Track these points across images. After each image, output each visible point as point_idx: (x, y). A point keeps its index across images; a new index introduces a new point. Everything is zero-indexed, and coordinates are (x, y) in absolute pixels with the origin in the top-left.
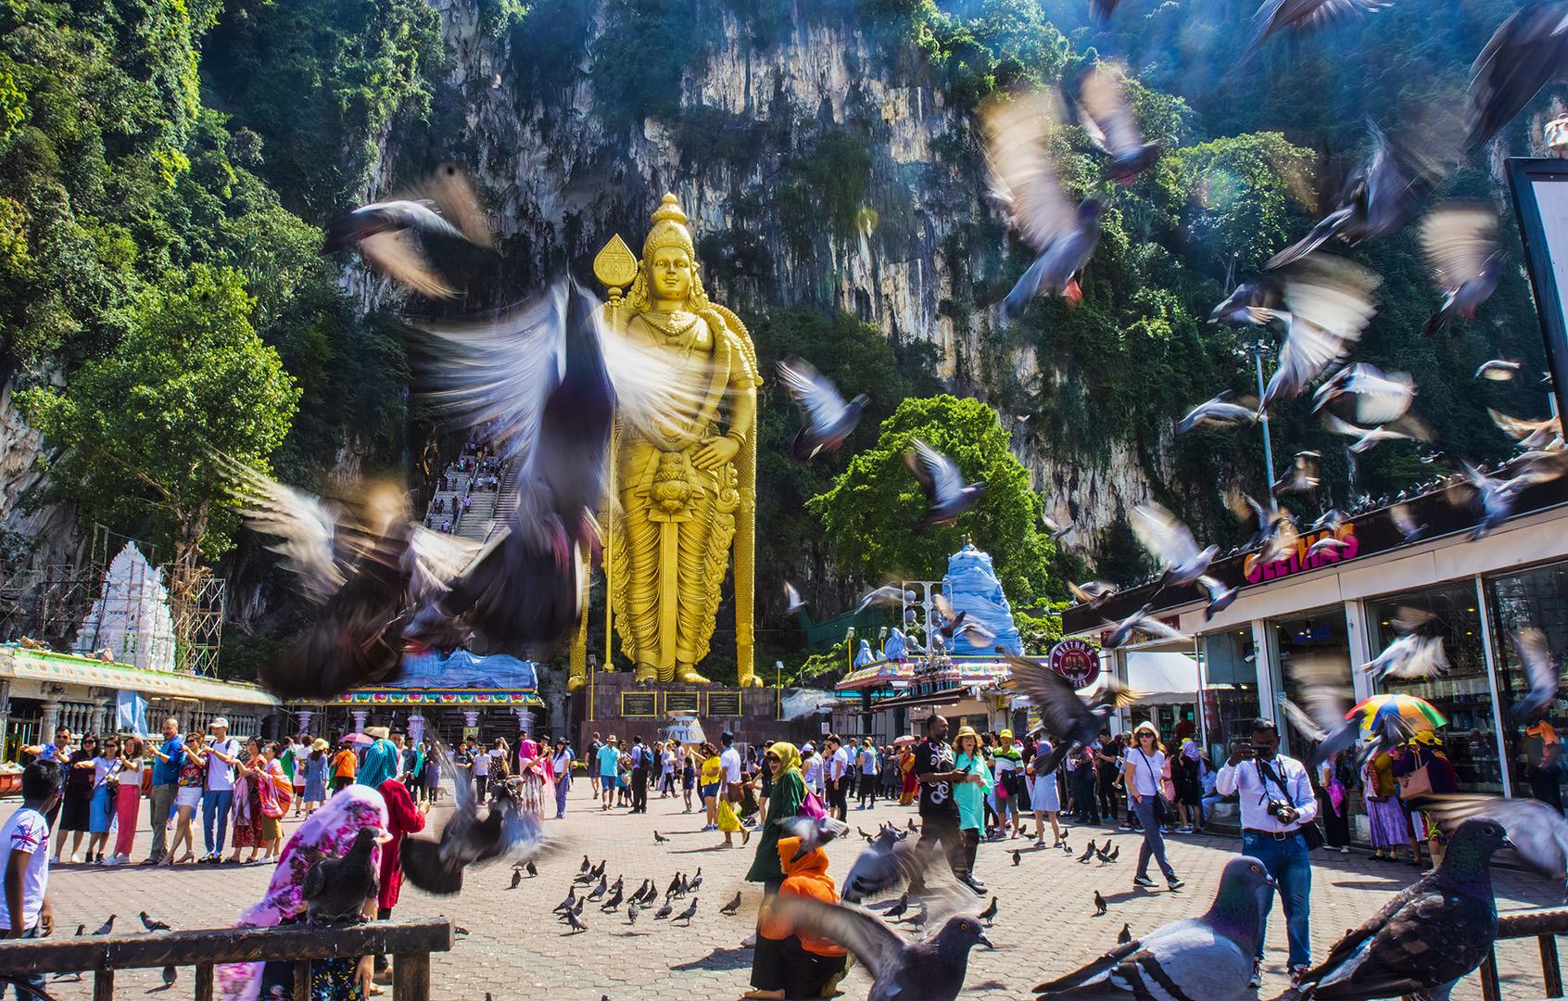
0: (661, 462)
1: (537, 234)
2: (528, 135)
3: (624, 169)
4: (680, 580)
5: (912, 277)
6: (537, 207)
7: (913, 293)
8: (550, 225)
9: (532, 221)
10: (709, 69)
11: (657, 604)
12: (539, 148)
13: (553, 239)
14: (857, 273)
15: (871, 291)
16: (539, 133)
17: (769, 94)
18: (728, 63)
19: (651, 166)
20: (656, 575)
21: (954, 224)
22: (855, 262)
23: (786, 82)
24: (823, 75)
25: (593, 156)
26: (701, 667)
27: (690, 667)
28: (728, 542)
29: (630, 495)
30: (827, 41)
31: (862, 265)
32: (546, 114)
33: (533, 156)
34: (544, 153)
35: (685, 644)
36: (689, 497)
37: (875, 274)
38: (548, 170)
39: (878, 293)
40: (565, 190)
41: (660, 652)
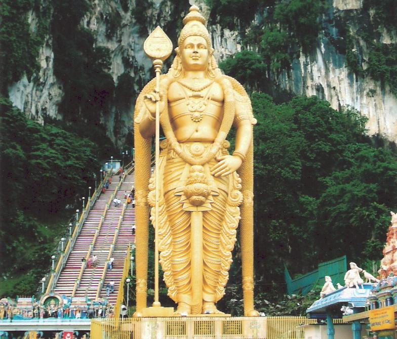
0: (190, 172)
1: (135, 73)
4: (204, 248)
6: (133, 57)
7: (351, 85)
8: (142, 68)
11: (190, 264)
12: (135, 24)
14: (316, 74)
15: (324, 85)
22: (315, 69)
27: (213, 304)
28: (236, 225)
29: (171, 195)
34: (137, 27)
35: (207, 290)
36: (209, 194)
39: (329, 86)
41: (192, 295)
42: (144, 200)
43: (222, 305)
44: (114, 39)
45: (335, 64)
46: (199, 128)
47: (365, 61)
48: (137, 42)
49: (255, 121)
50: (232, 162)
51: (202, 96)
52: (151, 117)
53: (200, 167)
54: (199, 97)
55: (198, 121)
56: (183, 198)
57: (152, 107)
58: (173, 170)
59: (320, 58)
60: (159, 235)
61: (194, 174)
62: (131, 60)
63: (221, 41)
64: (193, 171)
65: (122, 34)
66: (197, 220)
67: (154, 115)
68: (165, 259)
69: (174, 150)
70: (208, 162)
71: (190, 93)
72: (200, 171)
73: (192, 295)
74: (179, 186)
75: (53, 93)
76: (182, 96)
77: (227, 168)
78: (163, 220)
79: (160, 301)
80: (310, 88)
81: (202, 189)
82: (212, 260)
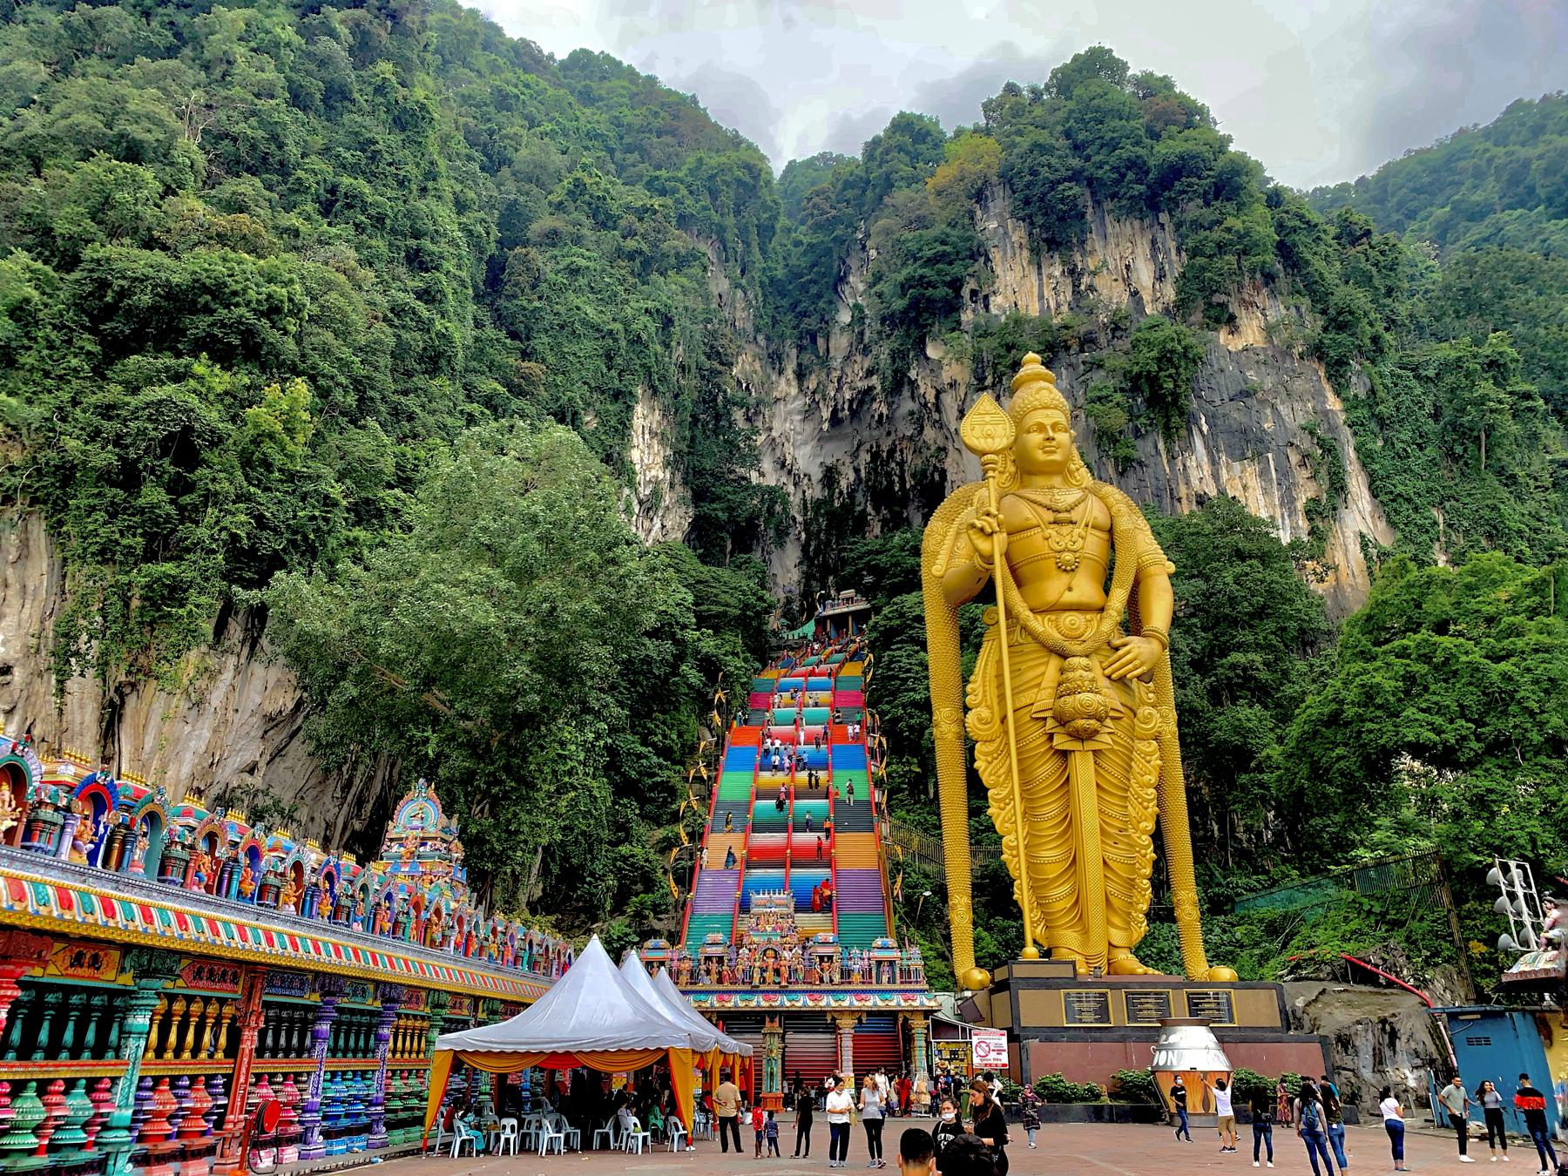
1: (795, 485)
3: (885, 412)
4: (1103, 832)
7: (1265, 492)
12: (795, 398)
14: (1194, 475)
16: (794, 383)
18: (1018, 268)
20: (1069, 822)
23: (1085, 280)
24: (1128, 267)
25: (851, 401)
26: (1143, 950)
28: (1153, 779)
30: (1128, 230)
31: (1199, 466)
33: (790, 407)
35: (1116, 920)
37: (1216, 476)
40: (822, 439)
42: (955, 728)
43: (1143, 950)
45: (1231, 456)
46: (1074, 583)
49: (1172, 568)
50: (1142, 650)
52: (978, 561)
53: (1084, 661)
56: (1050, 723)
57: (984, 545)
58: (1023, 667)
59: (1198, 443)
60: (997, 801)
61: (1071, 675)
64: (1074, 670)
65: (772, 416)
67: (989, 560)
69: (1024, 628)
70: (1096, 651)
71: (1050, 516)
72: (1087, 669)
73: (1085, 932)
74: (1043, 698)
75: (669, 524)
76: (1034, 522)
77: (1137, 662)
80: (1184, 501)
81: (1095, 705)
82: (1116, 854)
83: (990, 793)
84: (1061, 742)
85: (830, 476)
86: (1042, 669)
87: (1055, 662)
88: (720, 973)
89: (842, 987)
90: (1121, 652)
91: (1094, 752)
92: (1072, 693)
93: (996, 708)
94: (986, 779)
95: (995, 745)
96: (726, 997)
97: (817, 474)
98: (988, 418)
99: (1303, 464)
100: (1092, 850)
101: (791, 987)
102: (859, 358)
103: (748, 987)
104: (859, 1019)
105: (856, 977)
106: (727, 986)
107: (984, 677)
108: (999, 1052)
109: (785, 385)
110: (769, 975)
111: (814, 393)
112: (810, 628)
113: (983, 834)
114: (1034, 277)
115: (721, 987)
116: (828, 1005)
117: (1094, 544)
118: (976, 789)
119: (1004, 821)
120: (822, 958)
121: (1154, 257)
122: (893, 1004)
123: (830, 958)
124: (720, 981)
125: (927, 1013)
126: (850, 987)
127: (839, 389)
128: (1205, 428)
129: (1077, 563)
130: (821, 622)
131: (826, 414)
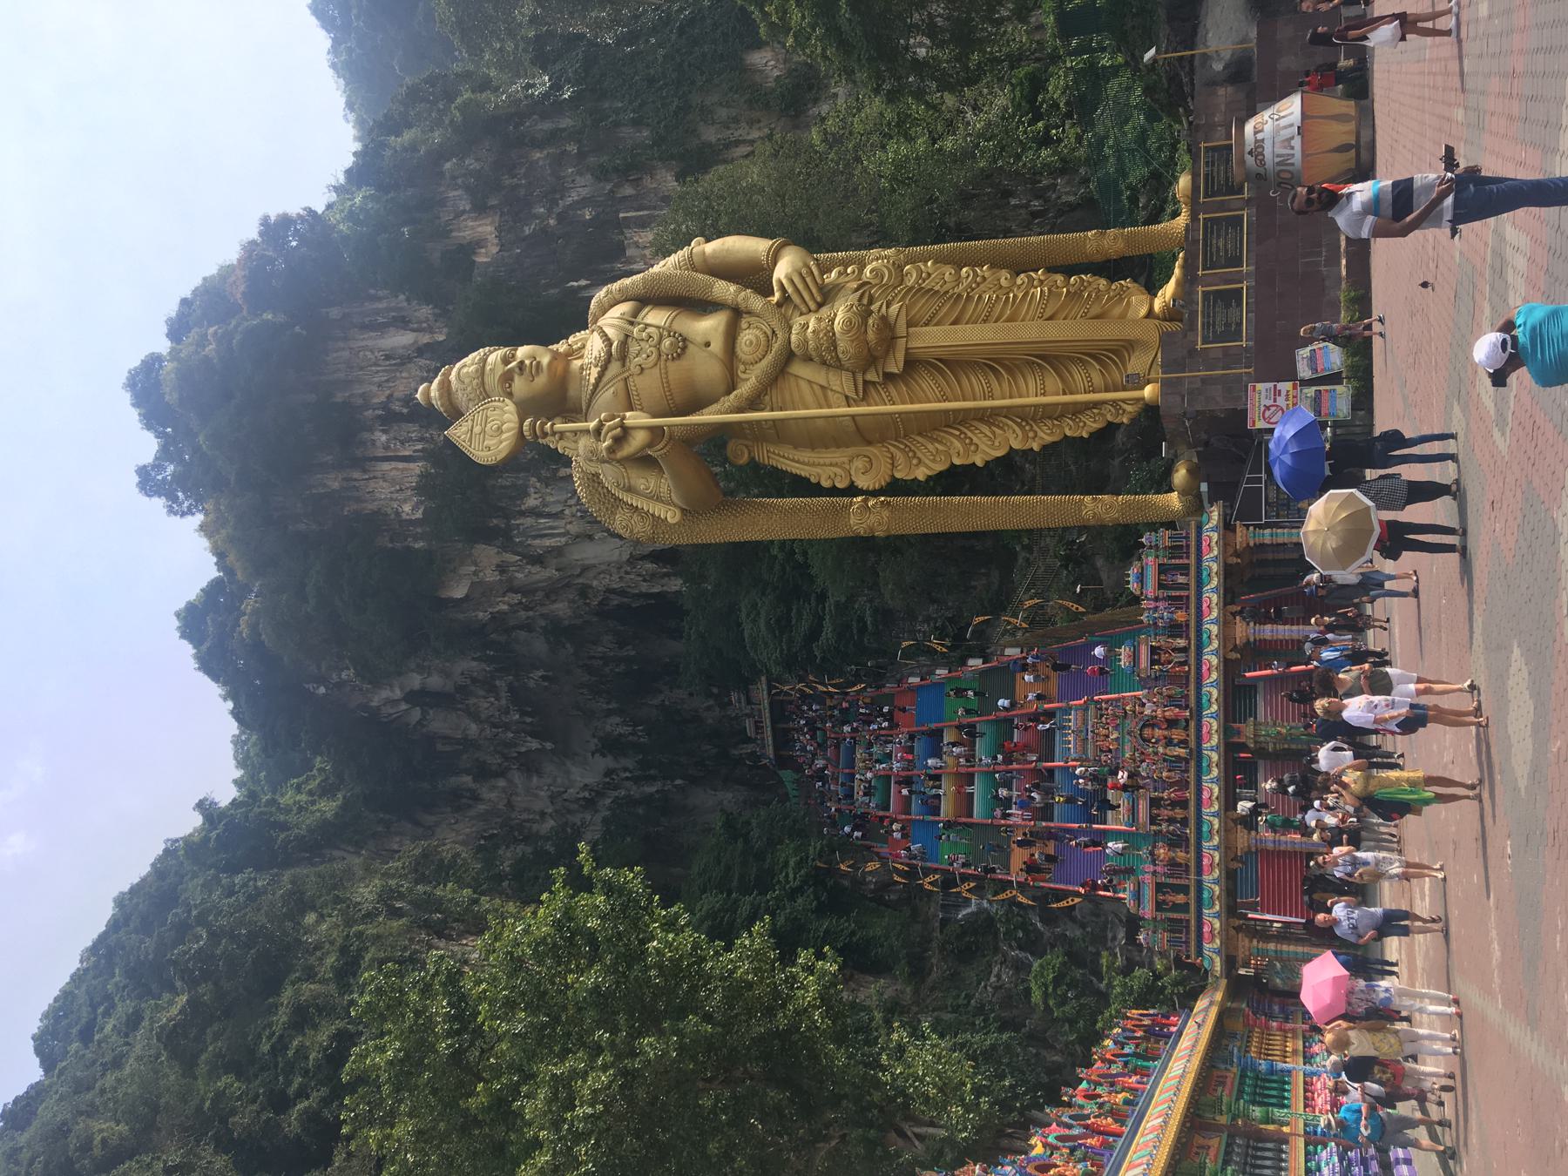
2: (493, 795)
3: (540, 673)
5: (643, 224)
8: (609, 773)
9: (600, 794)
10: (377, 512)
13: (626, 770)
17: (413, 430)
18: (372, 484)
19: (504, 595)
21: (580, 174)
23: (396, 407)
24: (388, 357)
25: (523, 714)
28: (948, 271)
30: (346, 354)
32: (467, 772)
34: (517, 777)
35: (1117, 311)
38: (539, 773)
44: (535, 827)
46: (699, 339)
47: (612, 191)
48: (549, 781)
51: (622, 337)
54: (624, 344)
55: (684, 340)
56: (872, 376)
61: (811, 344)
62: (587, 794)
63: (549, 516)
65: (527, 810)
66: (934, 338)
68: (1031, 434)
71: (615, 367)
76: (621, 384)
77: (804, 271)
78: (930, 447)
79: (1142, 388)
83: (957, 462)
84: (895, 367)
85: (611, 746)
86: (803, 384)
87: (798, 369)
88: (1173, 804)
89: (1193, 635)
90: (790, 290)
91: (910, 324)
92: (833, 343)
93: (851, 451)
94: (940, 467)
95: (898, 454)
96: (1205, 795)
97: (609, 762)
98: (477, 429)
99: (636, 182)
100: (1030, 331)
101: (1192, 703)
102: (472, 701)
103: (1193, 763)
104: (1234, 614)
105: (1180, 616)
106: (1190, 794)
107: (813, 465)
108: (1277, 393)
109: (492, 794)
110: (1177, 735)
111: (506, 758)
112: (787, 775)
113: (1004, 475)
114: (386, 466)
115: (1192, 804)
116: (1216, 652)
117: (656, 317)
118: (955, 480)
119: (992, 446)
120: (1153, 662)
121: (381, 328)
122: (1215, 567)
123: (1154, 650)
124: (1183, 804)
125: (1227, 526)
126: (1192, 624)
127: (507, 727)
128: (583, 282)
129: (671, 332)
130: (783, 761)
131: (534, 744)
